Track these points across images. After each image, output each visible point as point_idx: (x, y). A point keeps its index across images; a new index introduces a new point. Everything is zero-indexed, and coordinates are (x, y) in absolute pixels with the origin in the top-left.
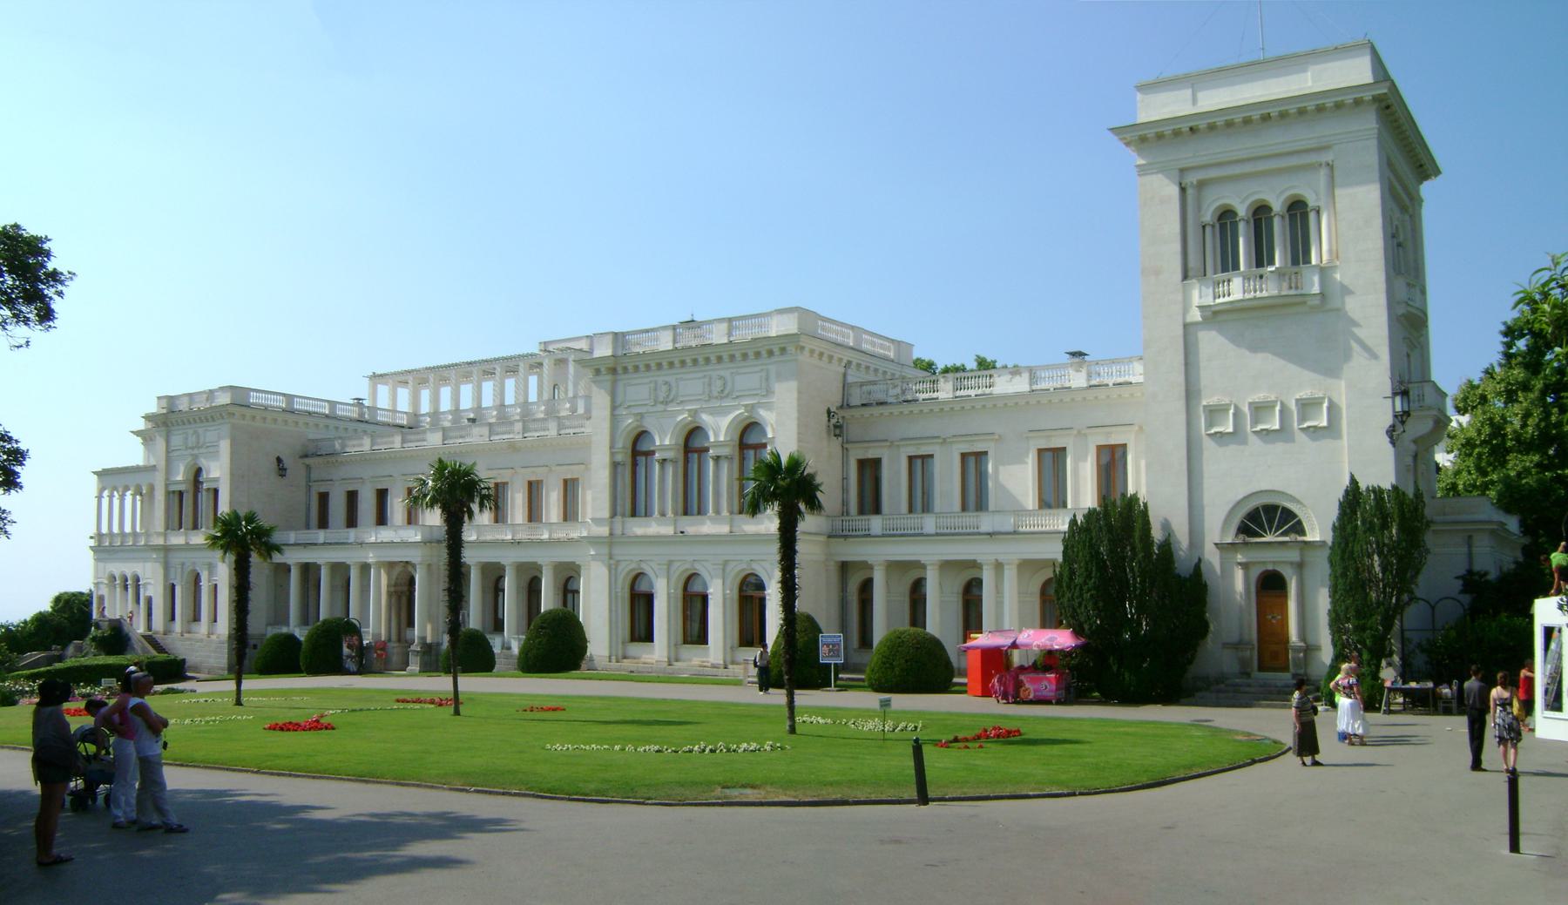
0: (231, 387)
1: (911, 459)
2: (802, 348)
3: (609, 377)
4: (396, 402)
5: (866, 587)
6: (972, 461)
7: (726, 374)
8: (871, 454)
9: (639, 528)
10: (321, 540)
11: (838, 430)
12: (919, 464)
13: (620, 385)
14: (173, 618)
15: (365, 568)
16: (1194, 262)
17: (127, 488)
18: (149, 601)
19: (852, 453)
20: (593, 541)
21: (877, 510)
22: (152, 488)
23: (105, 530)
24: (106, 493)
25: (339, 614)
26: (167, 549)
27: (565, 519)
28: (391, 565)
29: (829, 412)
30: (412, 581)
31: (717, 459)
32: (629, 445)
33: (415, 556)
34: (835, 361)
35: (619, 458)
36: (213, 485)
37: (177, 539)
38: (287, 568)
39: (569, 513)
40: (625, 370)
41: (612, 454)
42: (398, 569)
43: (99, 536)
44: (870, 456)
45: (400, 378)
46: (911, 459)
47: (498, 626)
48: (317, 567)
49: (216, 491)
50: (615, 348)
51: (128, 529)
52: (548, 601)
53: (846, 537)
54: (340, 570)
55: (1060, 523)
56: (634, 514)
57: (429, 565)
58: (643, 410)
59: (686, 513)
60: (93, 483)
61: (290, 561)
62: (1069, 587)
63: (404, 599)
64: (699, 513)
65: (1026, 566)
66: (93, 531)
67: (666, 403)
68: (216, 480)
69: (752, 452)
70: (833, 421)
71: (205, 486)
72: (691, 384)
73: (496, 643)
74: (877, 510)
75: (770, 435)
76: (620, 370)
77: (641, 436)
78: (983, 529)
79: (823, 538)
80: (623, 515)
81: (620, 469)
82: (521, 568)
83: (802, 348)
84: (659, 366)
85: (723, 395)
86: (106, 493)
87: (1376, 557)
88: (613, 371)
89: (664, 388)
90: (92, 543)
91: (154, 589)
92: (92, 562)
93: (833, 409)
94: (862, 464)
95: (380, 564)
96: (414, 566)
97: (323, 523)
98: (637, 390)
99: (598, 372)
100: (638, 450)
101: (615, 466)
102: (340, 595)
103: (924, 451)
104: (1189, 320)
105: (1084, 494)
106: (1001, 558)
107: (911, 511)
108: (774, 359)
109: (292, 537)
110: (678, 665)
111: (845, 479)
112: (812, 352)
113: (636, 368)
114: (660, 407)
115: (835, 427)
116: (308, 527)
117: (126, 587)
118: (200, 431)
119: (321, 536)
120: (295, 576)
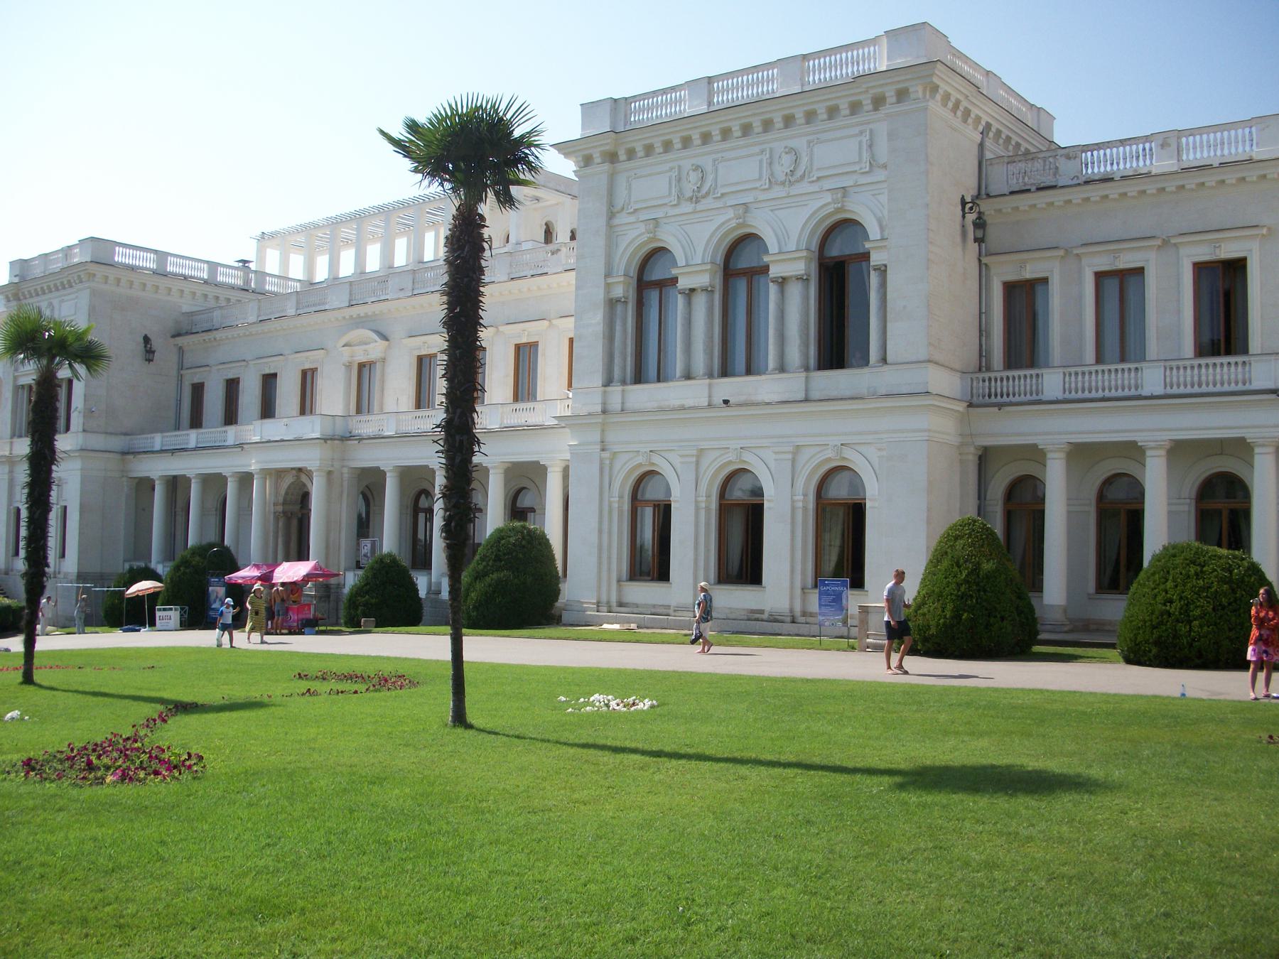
0: (93, 239)
1: (1099, 276)
3: (606, 166)
7: (800, 143)
9: (645, 395)
10: (192, 444)
12: (1120, 287)
13: (621, 181)
14: (17, 554)
15: (245, 480)
19: (993, 271)
25: (212, 537)
28: (279, 474)
29: (964, 203)
30: (305, 497)
31: (782, 282)
32: (633, 272)
33: (310, 459)
35: (618, 292)
40: (631, 154)
41: (608, 286)
42: (288, 480)
44: (1028, 274)
46: (1099, 276)
47: (423, 562)
50: (614, 121)
52: (493, 518)
53: (1000, 406)
54: (214, 482)
56: (639, 378)
57: (330, 473)
58: (659, 214)
59: (725, 372)
63: (295, 522)
64: (749, 371)
67: (695, 199)
70: (971, 217)
72: (739, 169)
76: (622, 157)
78: (1256, 385)
79: (961, 407)
80: (624, 382)
81: (619, 308)
83: (935, 89)
84: (686, 142)
85: (792, 178)
88: (612, 157)
89: (694, 177)
93: (968, 199)
94: (1013, 290)
95: (266, 473)
96: (309, 474)
97: (196, 421)
98: (649, 185)
99: (587, 161)
100: (650, 280)
101: (612, 304)
102: (213, 521)
103: (1126, 261)
107: (1099, 359)
108: (884, 110)
109: (158, 441)
111: (983, 314)
112: (947, 97)
113: (649, 150)
114: (687, 207)
116: (177, 428)
118: (55, 302)
119: (192, 438)
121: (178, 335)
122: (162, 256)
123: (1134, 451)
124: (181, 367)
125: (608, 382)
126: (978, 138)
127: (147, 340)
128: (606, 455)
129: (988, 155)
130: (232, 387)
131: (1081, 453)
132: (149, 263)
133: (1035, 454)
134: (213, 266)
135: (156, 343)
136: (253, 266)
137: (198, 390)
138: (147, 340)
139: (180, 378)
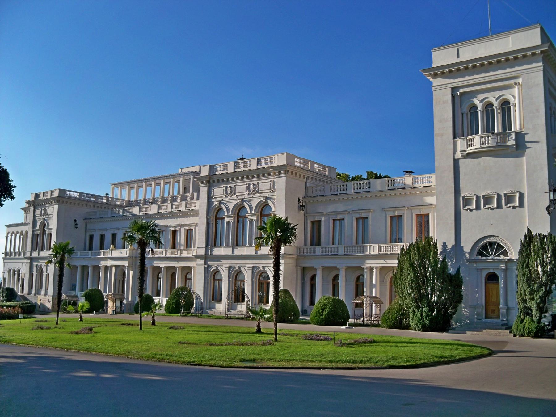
2: (288, 171)
4: (121, 195)
5: (313, 278)
6: (361, 222)
8: (316, 219)
11: (302, 207)
16: (459, 131)
17: (17, 232)
18: (23, 280)
20: (199, 257)
21: (319, 244)
22: (27, 232)
23: (8, 250)
24: (10, 235)
26: (31, 259)
27: (187, 247)
28: (116, 267)
29: (299, 199)
33: (126, 263)
34: (302, 177)
36: (50, 231)
37: (35, 254)
38: (76, 267)
39: (188, 245)
43: (6, 254)
45: (122, 184)
48: (88, 267)
49: (51, 234)
51: (17, 250)
55: (397, 249)
60: (5, 230)
61: (77, 265)
62: (400, 279)
65: (383, 270)
66: (4, 251)
68: (51, 229)
69: (266, 218)
71: (47, 232)
72: (241, 187)
73: (157, 300)
74: (319, 244)
75: (273, 210)
77: (220, 210)
82: (168, 268)
83: (288, 171)
86: (10, 235)
87: (539, 266)
90: (3, 256)
91: (25, 274)
92: (2, 264)
94: (313, 223)
95: (111, 266)
102: (96, 279)
104: (456, 157)
105: (410, 237)
106: (372, 266)
110: (233, 312)
115: (302, 206)
116: (85, 249)
117: (14, 275)
120: (79, 270)
121: (85, 219)
122: (81, 194)
123: (336, 268)
124: (86, 230)
125: (207, 245)
126: (305, 180)
127: (75, 221)
128: (206, 266)
129: (308, 185)
130: (102, 236)
131: (326, 269)
132: (77, 196)
133: (313, 269)
134: (97, 196)
135: (78, 222)
136: (110, 196)
137: (91, 237)
138: (75, 221)
139: (86, 232)
